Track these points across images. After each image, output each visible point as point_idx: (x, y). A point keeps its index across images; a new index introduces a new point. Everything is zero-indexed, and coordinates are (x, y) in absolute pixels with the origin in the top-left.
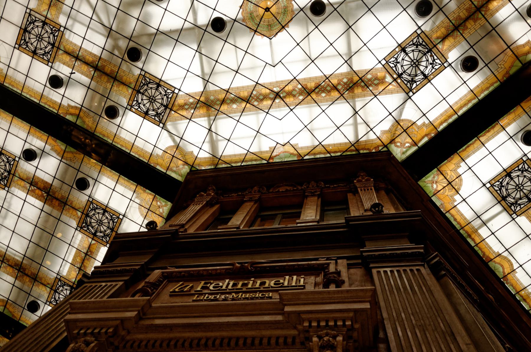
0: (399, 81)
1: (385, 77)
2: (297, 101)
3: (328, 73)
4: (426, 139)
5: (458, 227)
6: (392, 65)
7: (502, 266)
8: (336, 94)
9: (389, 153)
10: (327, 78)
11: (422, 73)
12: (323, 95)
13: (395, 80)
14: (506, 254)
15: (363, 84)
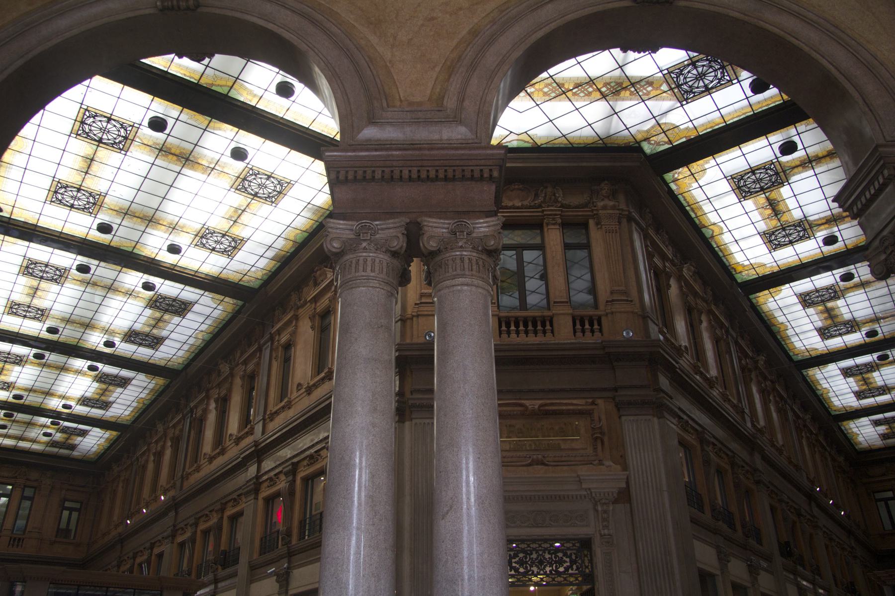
0: (676, 90)
1: (661, 85)
2: (547, 98)
3: (593, 73)
4: (684, 140)
5: (685, 204)
6: (673, 75)
7: (713, 231)
8: (598, 95)
9: (640, 149)
10: (591, 80)
11: (706, 86)
12: (582, 95)
13: (671, 89)
14: (722, 224)
15: (633, 89)
